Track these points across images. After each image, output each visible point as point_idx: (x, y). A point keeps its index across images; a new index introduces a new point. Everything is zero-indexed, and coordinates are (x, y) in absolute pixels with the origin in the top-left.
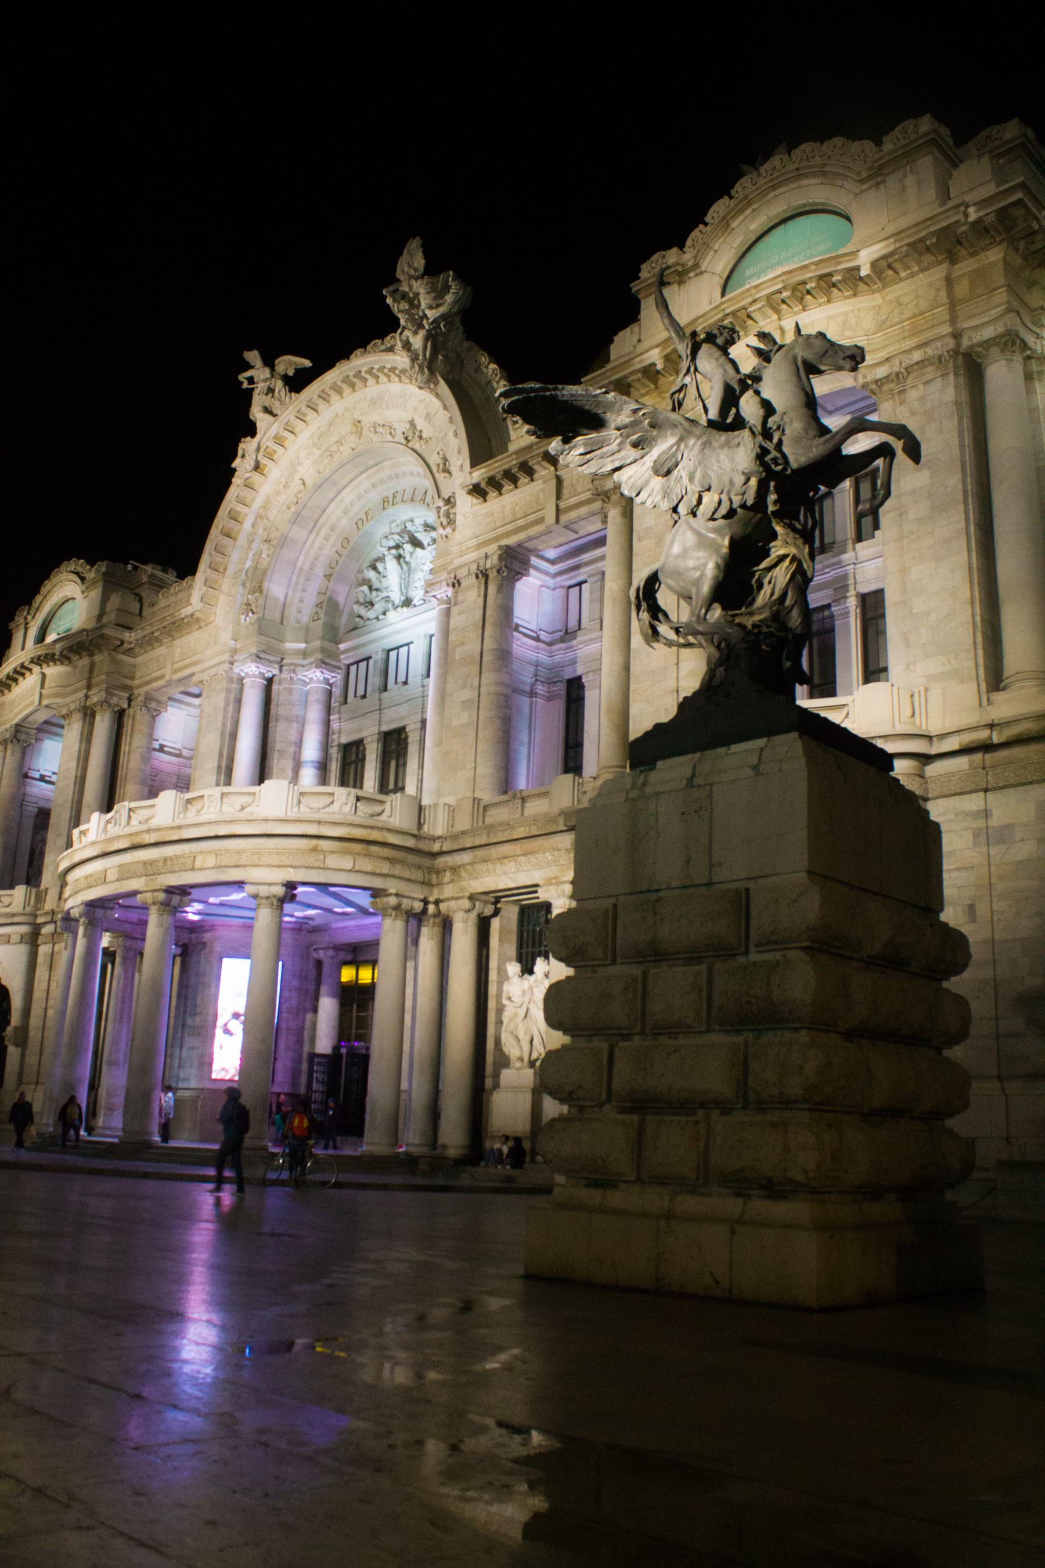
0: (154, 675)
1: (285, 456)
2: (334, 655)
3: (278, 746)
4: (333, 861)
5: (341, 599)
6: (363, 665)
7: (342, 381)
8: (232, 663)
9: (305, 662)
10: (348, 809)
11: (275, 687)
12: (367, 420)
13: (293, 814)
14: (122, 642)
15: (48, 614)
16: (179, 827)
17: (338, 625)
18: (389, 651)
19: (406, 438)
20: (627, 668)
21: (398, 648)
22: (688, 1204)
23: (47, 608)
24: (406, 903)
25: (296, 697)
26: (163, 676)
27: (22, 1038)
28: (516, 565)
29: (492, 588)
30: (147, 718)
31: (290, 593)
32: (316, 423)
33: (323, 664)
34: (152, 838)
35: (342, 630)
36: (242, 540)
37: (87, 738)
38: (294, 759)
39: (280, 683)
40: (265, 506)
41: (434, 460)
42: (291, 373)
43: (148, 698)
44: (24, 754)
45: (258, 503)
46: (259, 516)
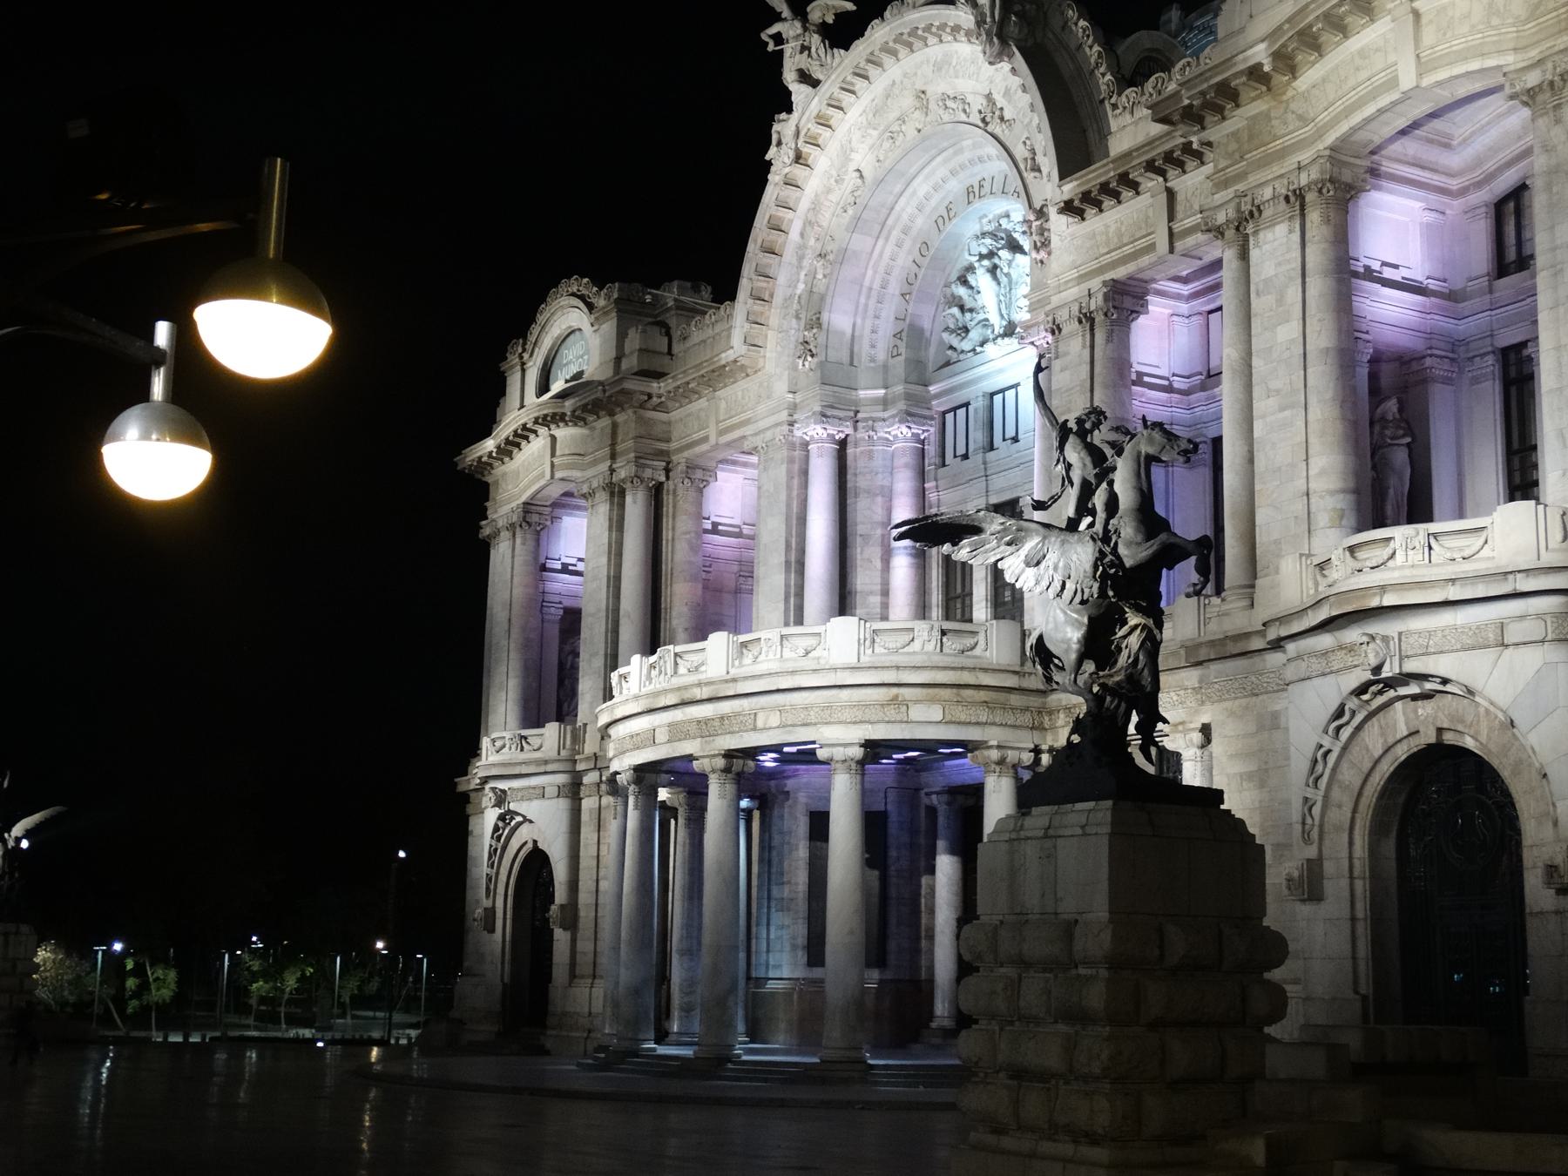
0: (695, 437)
1: (833, 141)
2: (924, 402)
3: (861, 529)
4: (917, 712)
5: (927, 325)
6: (961, 412)
7: (895, 41)
8: (791, 424)
9: (886, 415)
10: (930, 647)
11: (850, 451)
12: (936, 89)
13: (866, 659)
14: (650, 396)
15: (550, 350)
16: (734, 680)
17: (925, 362)
18: (992, 395)
19: (983, 120)
21: (1003, 391)
22: (1046, 1147)
23: (547, 343)
24: (1012, 756)
25: (878, 462)
26: (705, 439)
27: (570, 917)
28: (1128, 302)
30: (692, 494)
31: (859, 321)
32: (869, 93)
33: (909, 416)
34: (705, 693)
35: (931, 367)
36: (789, 255)
37: (617, 524)
38: (883, 545)
39: (856, 446)
40: (815, 207)
41: (1020, 152)
42: (830, 19)
43: (691, 467)
44: (538, 541)
45: (804, 205)
46: (808, 223)
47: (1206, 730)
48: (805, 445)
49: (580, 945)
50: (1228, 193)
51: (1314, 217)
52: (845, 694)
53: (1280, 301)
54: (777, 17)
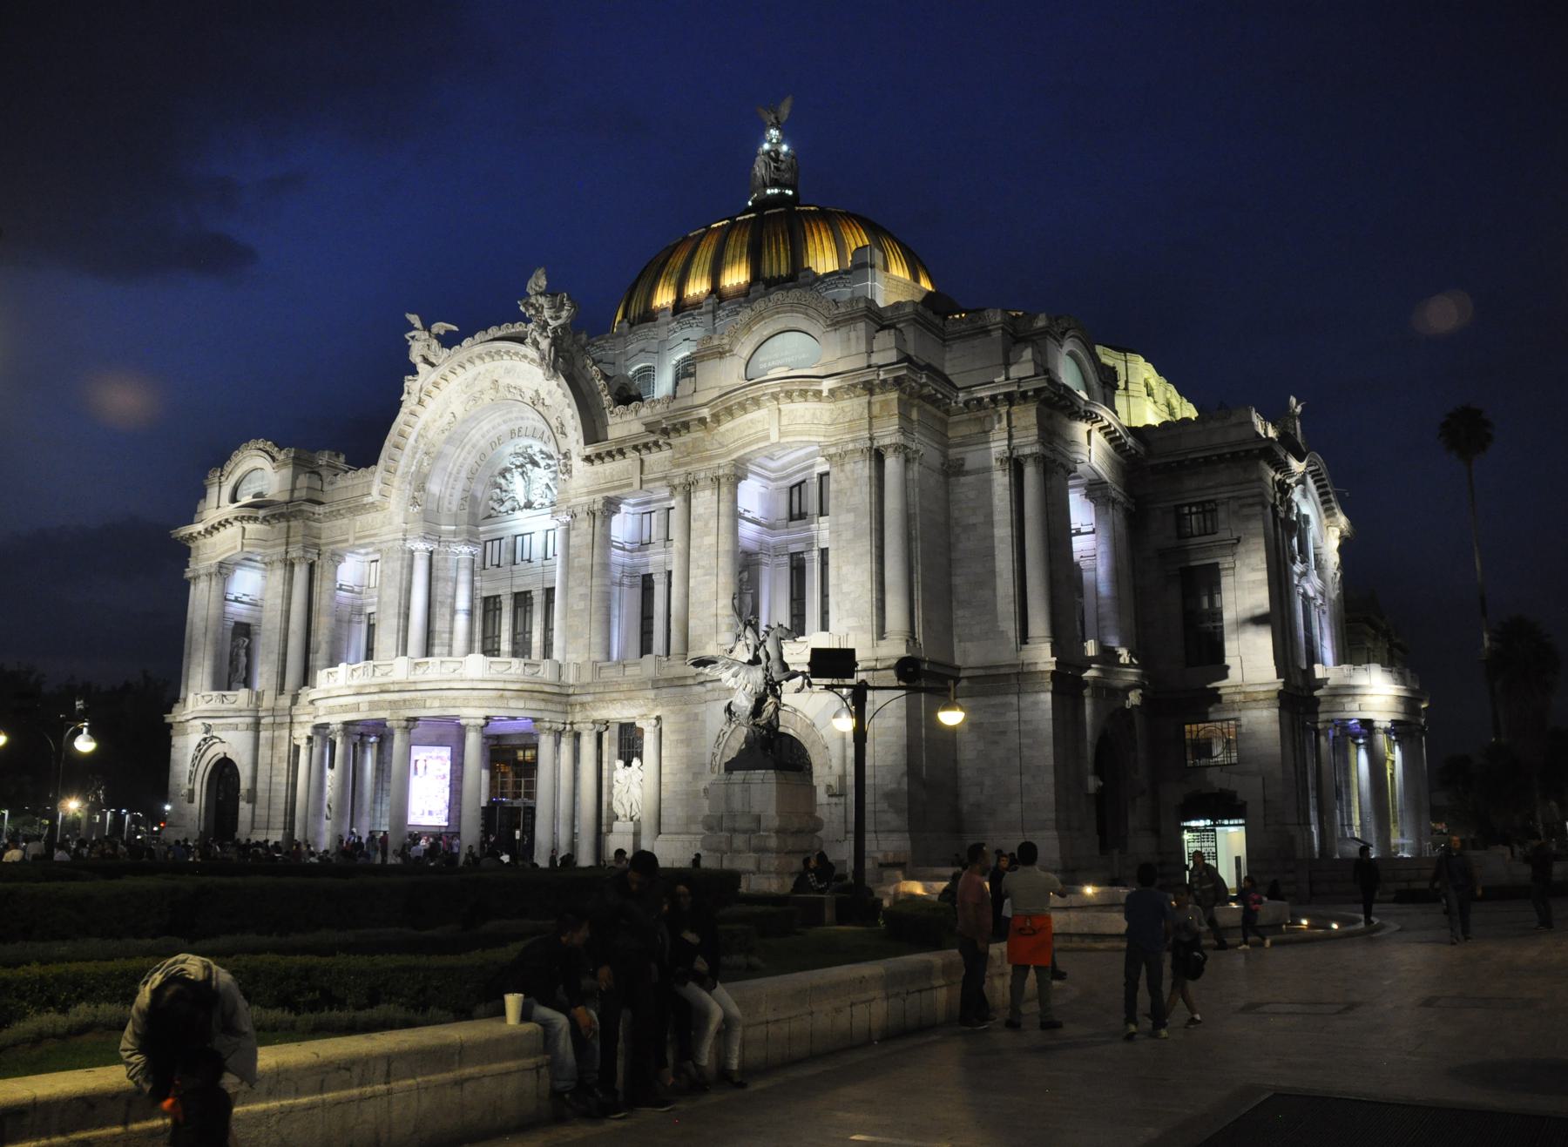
4: (512, 704)
5: (479, 495)
12: (504, 381)
13: (487, 676)
17: (481, 513)
20: (687, 596)
24: (555, 726)
25: (451, 564)
27: (252, 797)
29: (598, 523)
33: (469, 542)
34: (397, 687)
36: (408, 450)
37: (289, 581)
40: (425, 428)
43: (334, 554)
45: (419, 426)
46: (420, 435)
47: (658, 719)
48: (412, 552)
49: (257, 812)
50: (682, 470)
51: (724, 490)
52: (475, 693)
53: (706, 525)
54: (412, 328)
